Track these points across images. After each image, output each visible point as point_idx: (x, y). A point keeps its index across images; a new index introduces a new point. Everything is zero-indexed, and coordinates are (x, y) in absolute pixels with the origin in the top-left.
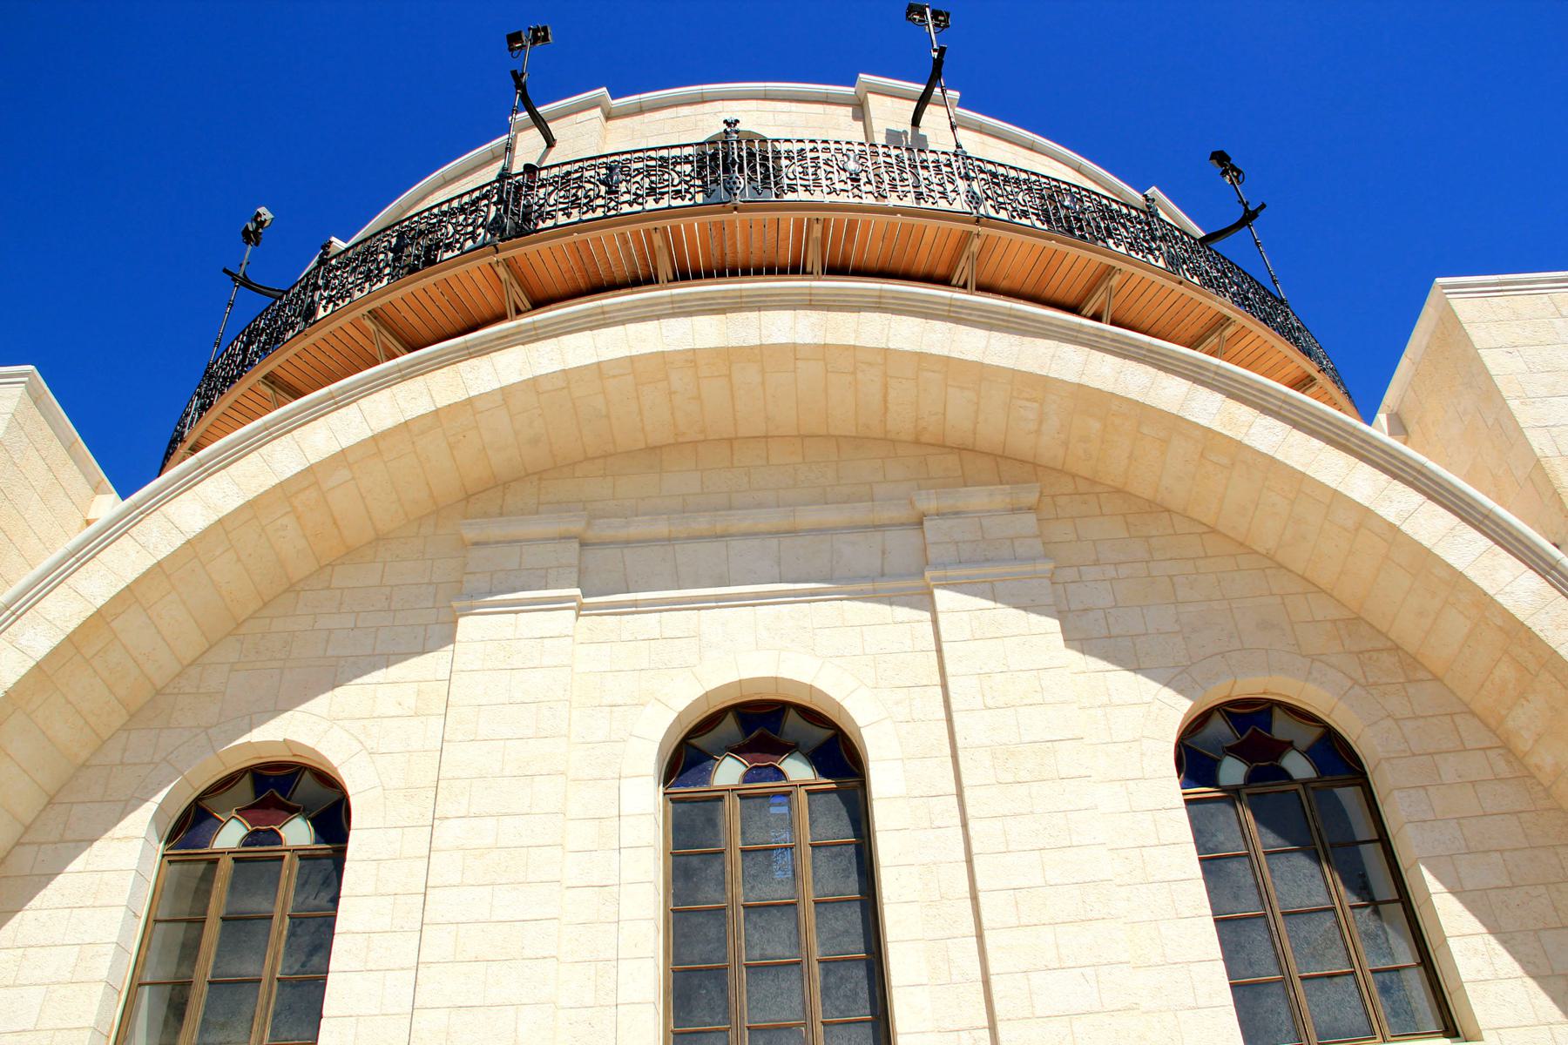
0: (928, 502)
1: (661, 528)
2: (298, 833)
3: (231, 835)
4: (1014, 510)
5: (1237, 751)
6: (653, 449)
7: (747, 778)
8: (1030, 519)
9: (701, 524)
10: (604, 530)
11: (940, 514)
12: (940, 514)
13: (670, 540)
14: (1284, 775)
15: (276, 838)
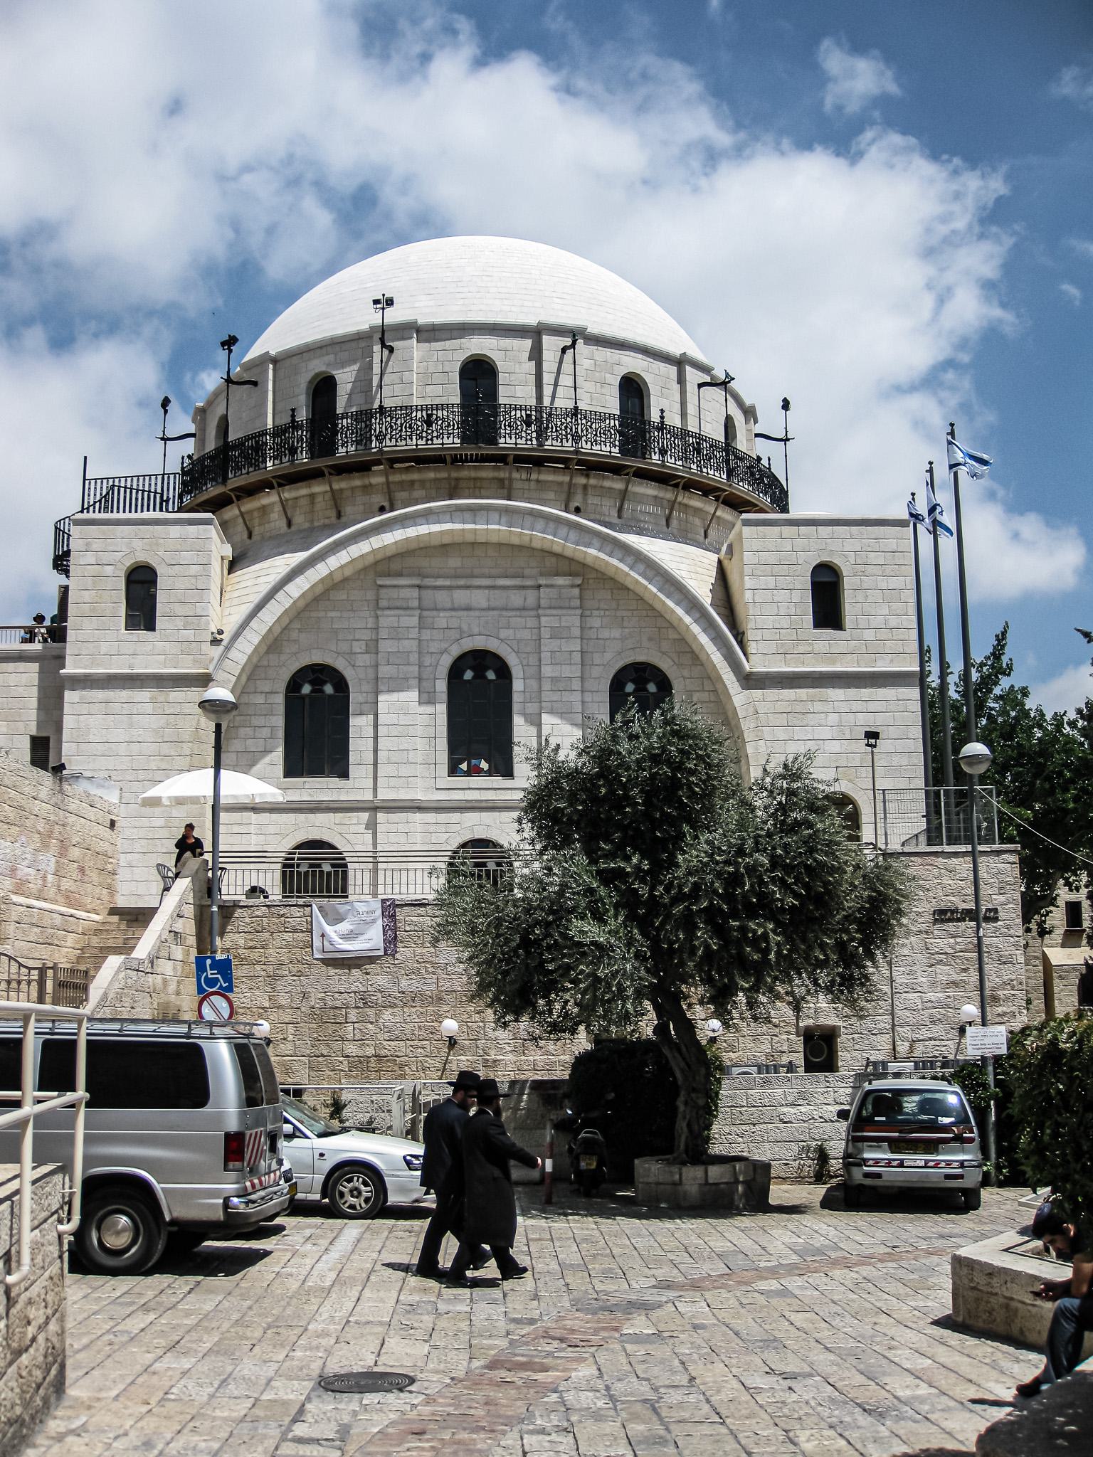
0: (542, 581)
1: (447, 583)
2: (329, 689)
3: (306, 689)
4: (573, 586)
5: (633, 681)
6: (444, 546)
7: (474, 677)
8: (576, 591)
9: (462, 582)
10: (428, 582)
11: (547, 586)
12: (547, 586)
13: (449, 588)
14: (646, 690)
15: (322, 691)
